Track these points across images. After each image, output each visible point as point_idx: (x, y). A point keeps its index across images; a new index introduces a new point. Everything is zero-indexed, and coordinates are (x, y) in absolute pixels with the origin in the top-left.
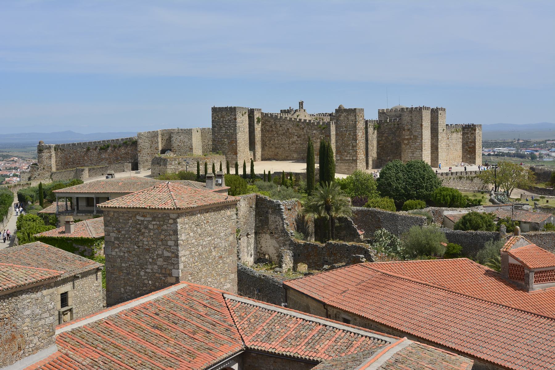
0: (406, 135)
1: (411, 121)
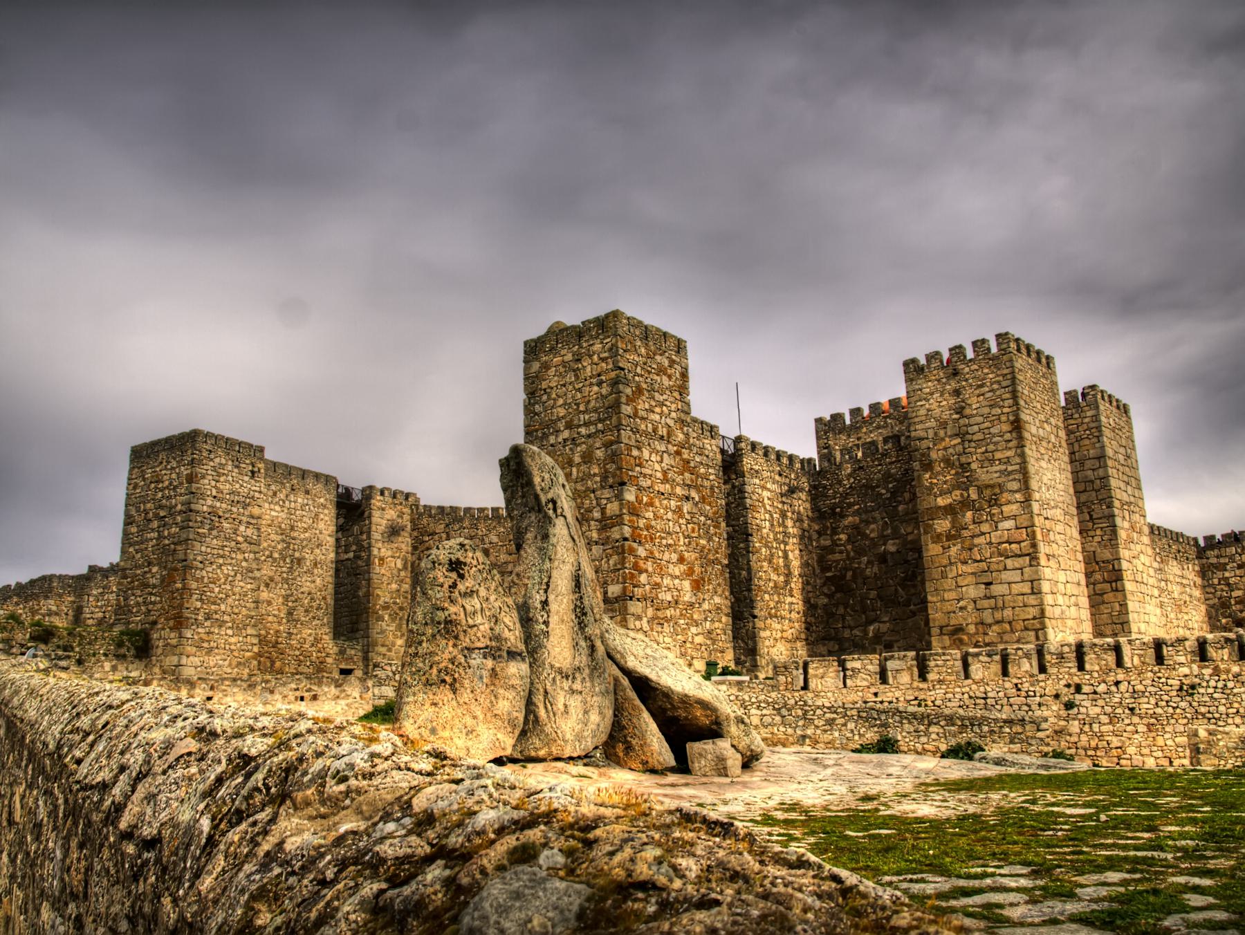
0: (938, 490)
1: (960, 411)
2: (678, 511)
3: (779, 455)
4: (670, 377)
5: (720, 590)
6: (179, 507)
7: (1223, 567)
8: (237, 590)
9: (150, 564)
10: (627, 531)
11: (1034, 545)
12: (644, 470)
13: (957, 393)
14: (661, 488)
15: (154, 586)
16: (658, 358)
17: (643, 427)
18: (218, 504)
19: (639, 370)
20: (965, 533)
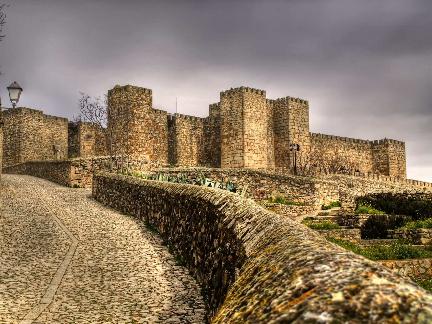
0: (225, 131)
3: (191, 118)
4: (145, 101)
5: (164, 158)
6: (17, 131)
7: (378, 152)
8: (35, 157)
9: (8, 149)
10: (129, 143)
11: (243, 147)
13: (231, 103)
14: (141, 131)
15: (10, 156)
16: (142, 96)
18: (29, 130)
19: (135, 100)
20: (230, 143)
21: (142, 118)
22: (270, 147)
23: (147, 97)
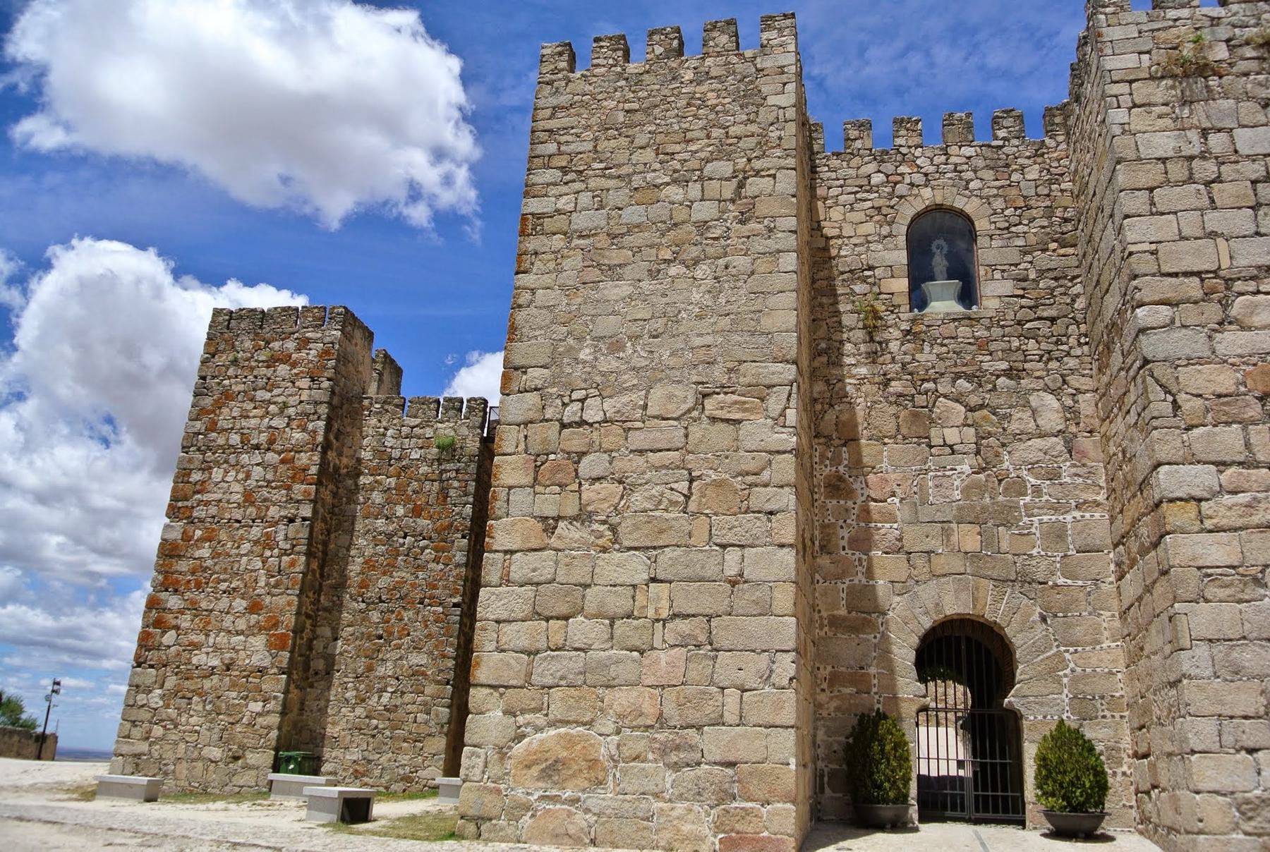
2: (267, 542)
12: (206, 497)
17: (221, 441)
21: (257, 447)
22: (1053, 475)
23: (304, 343)
